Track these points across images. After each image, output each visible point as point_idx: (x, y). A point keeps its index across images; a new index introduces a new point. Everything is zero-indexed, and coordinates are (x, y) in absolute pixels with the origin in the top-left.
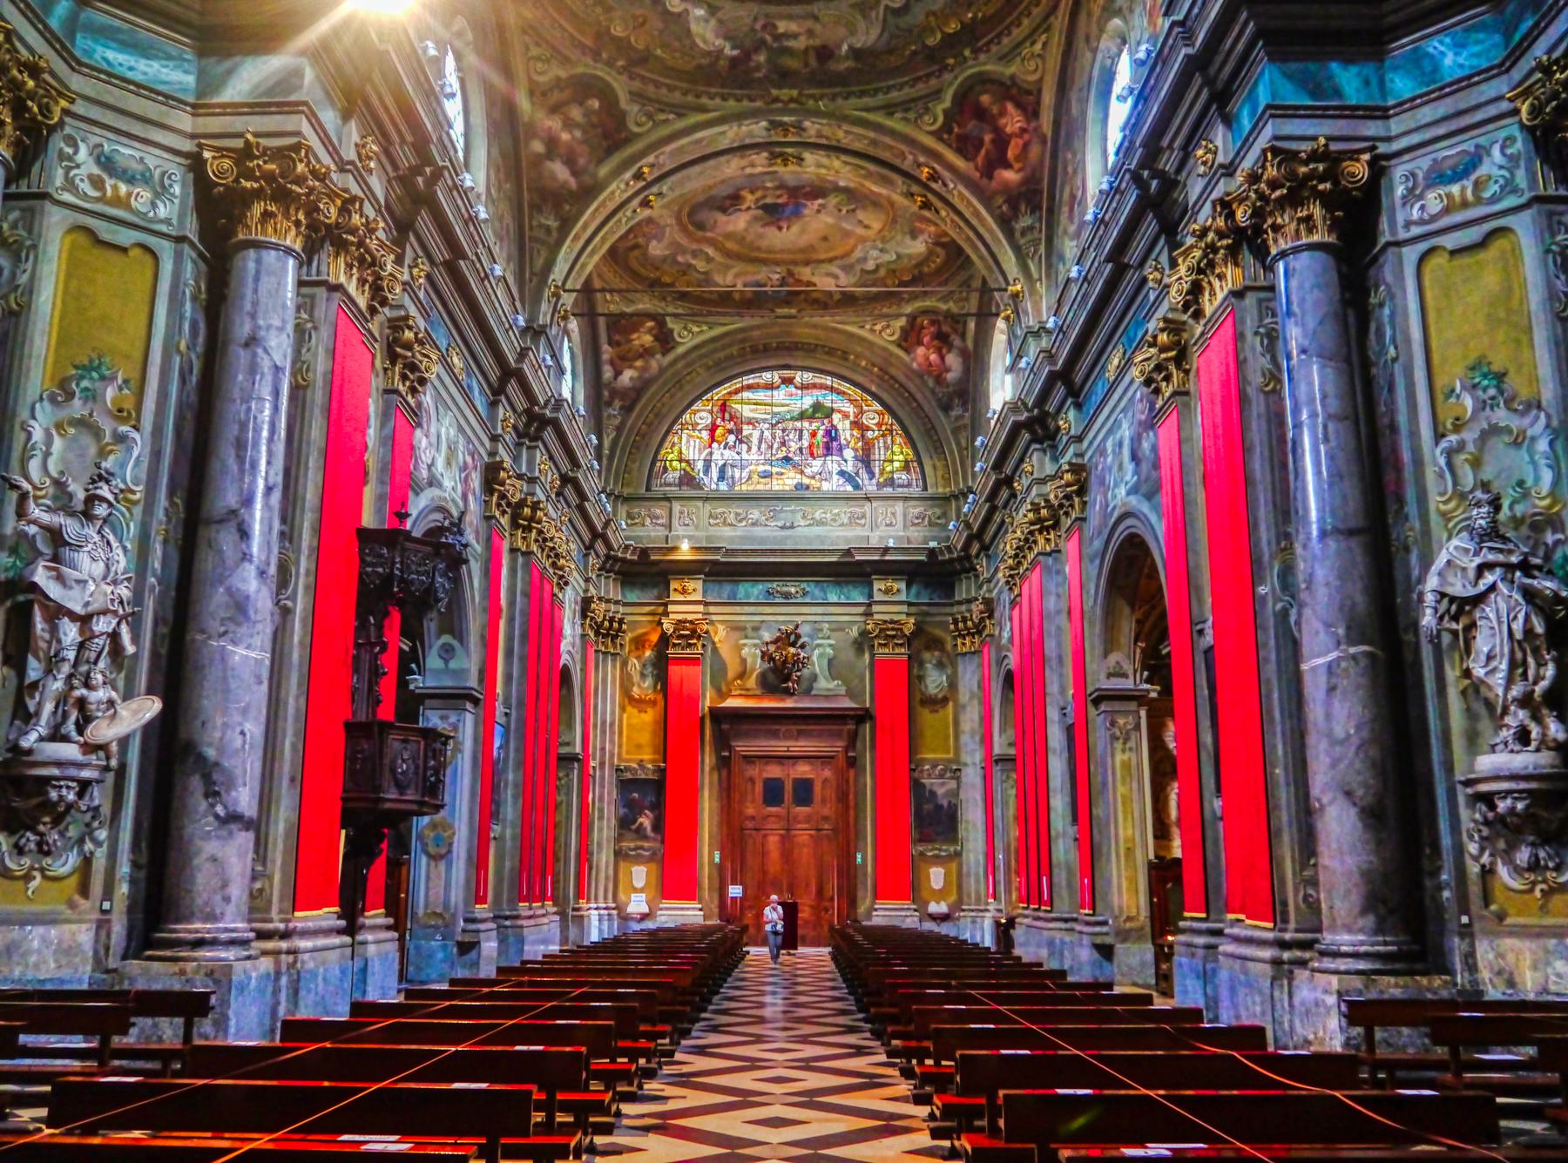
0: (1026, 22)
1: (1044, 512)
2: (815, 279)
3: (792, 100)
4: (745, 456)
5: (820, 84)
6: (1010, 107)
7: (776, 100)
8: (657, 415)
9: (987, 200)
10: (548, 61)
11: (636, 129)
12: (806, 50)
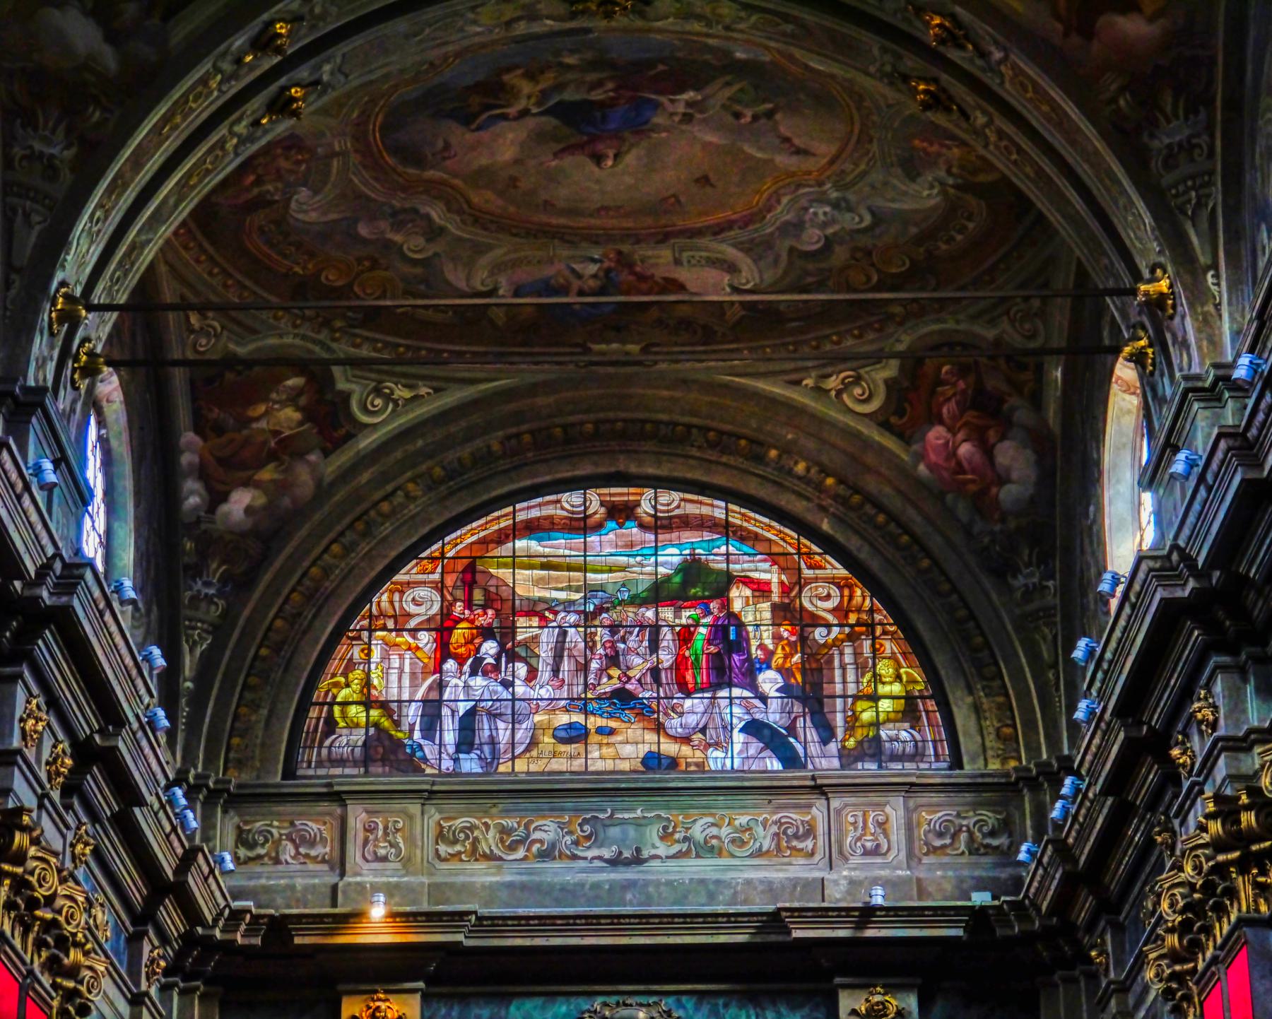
1: (1248, 819)
2: (683, 274)
4: (520, 689)
8: (309, 597)
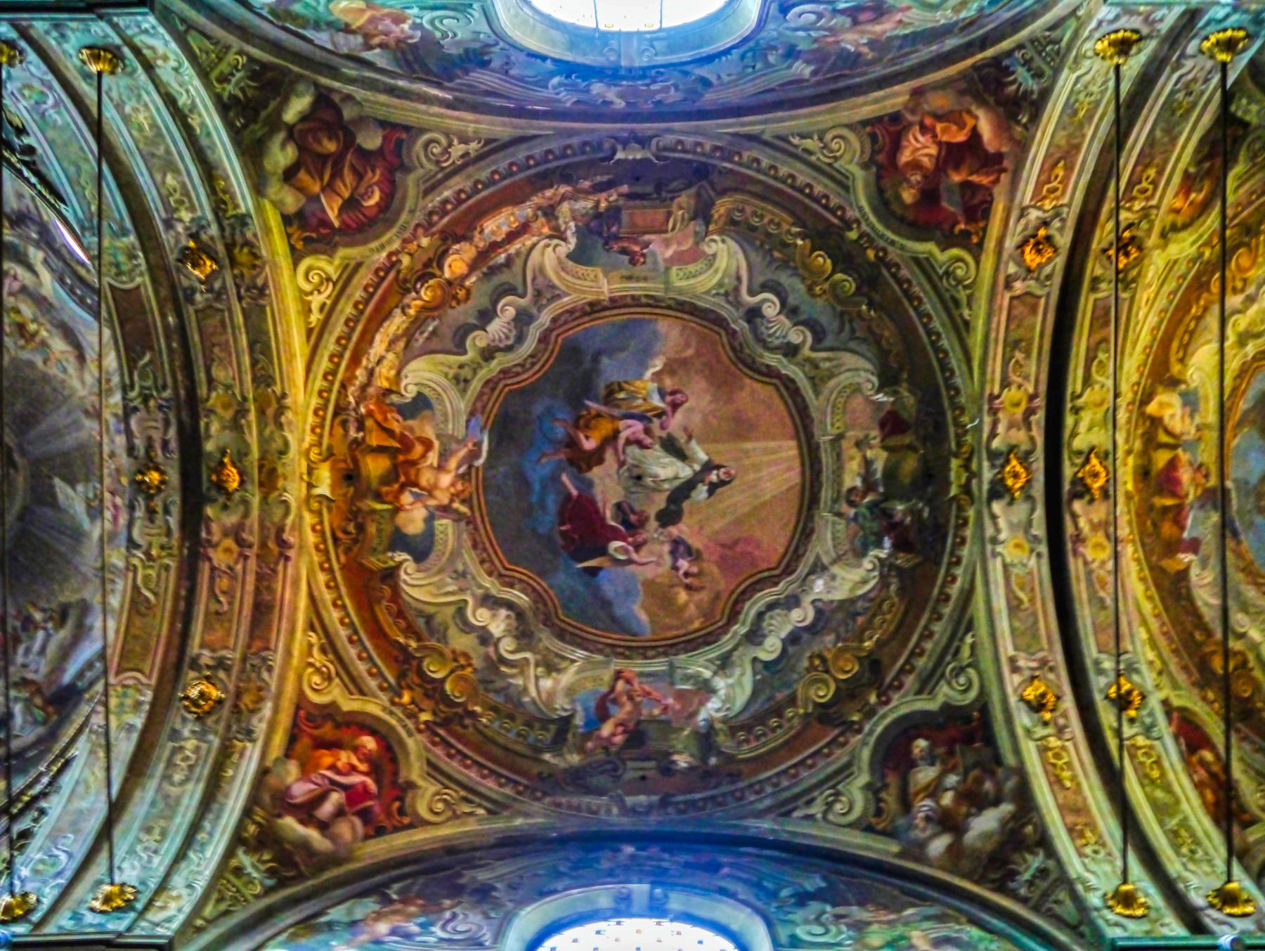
0: (784, 171)
3: (966, 466)
5: (940, 427)
6: (905, 157)
7: (966, 489)
9: (1023, 147)
10: (837, 794)
11: (973, 694)
12: (885, 448)
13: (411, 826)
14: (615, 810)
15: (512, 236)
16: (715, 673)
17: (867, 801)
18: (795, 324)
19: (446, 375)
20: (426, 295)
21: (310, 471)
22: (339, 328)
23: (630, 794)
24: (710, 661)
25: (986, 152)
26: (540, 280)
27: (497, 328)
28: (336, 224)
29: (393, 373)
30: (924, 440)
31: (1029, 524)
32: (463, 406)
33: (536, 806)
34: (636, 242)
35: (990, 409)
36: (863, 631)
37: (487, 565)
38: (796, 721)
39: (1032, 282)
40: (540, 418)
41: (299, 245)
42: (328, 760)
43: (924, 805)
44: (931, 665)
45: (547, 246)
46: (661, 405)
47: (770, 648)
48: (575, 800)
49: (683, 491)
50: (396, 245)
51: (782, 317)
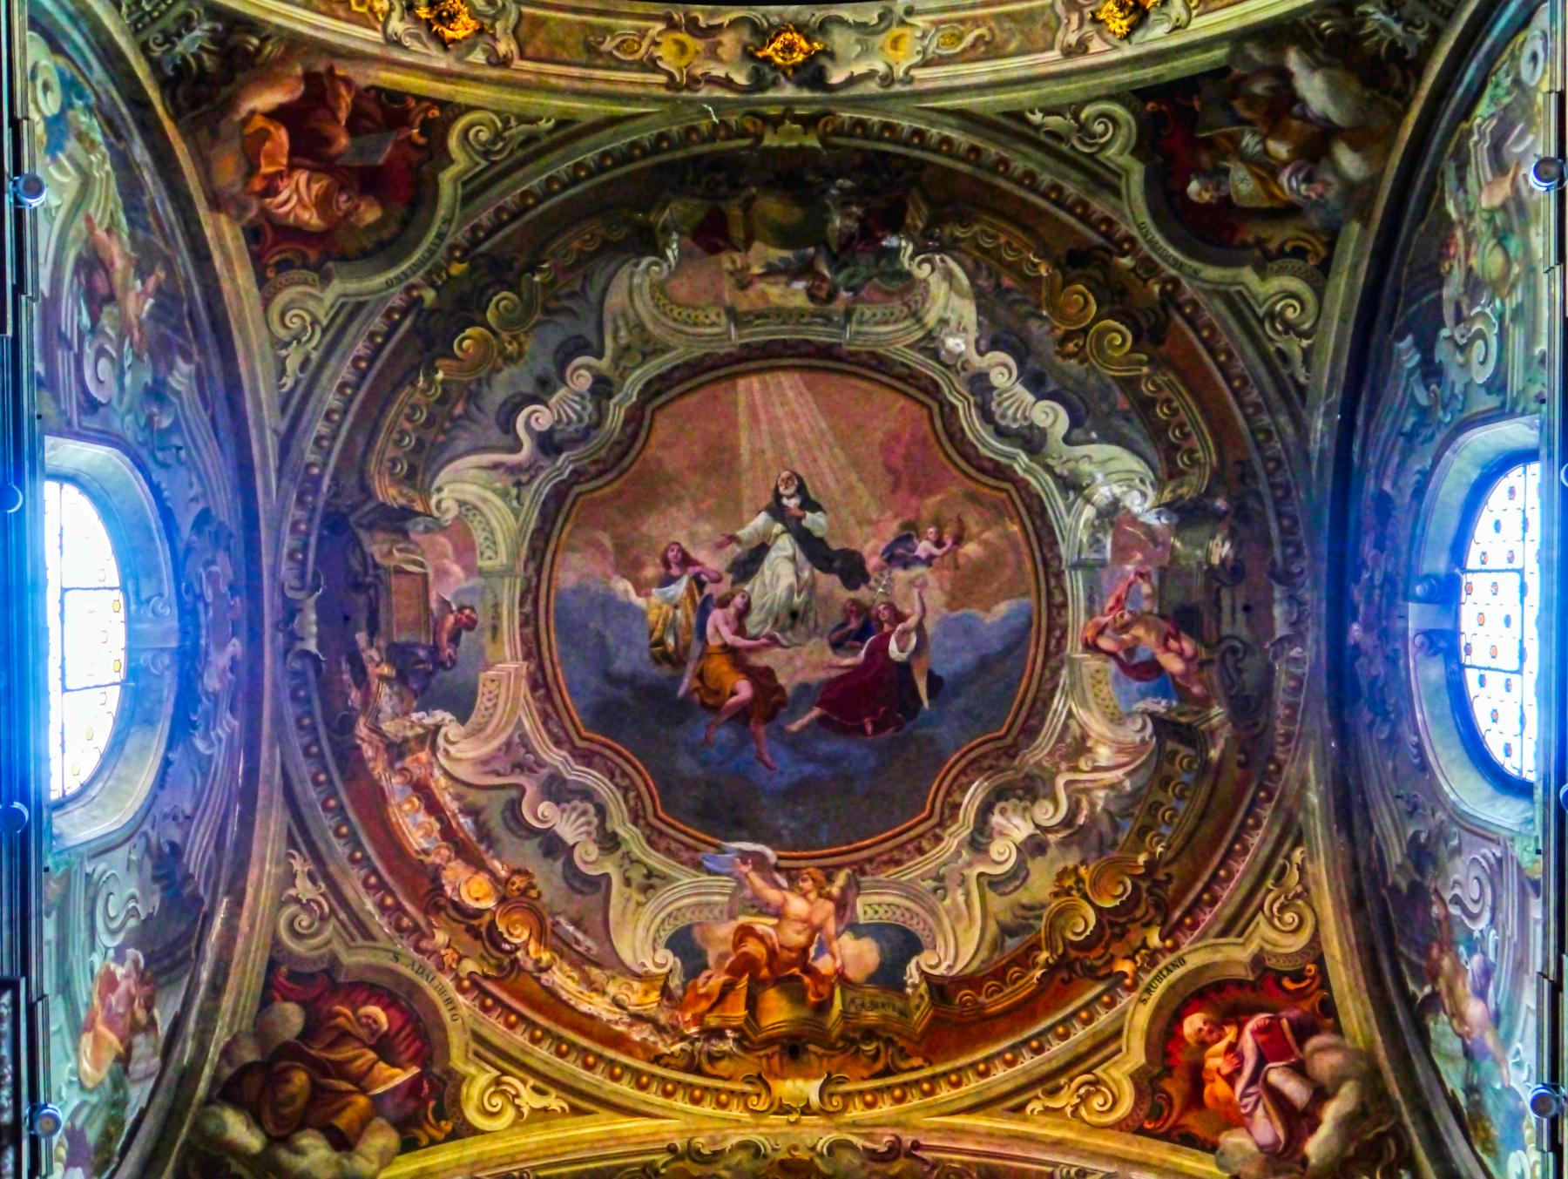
0: (332, 400)
3: (776, 122)
5: (717, 162)
6: (311, 218)
7: (809, 122)
9: (295, 44)
10: (1272, 316)
12: (747, 246)
13: (1320, 961)
14: (1296, 652)
15: (433, 807)
16: (1088, 501)
17: (1280, 272)
18: (563, 381)
19: (639, 904)
20: (520, 935)
21: (784, 1110)
22: (571, 1067)
23: (1271, 631)
24: (1069, 510)
25: (303, 98)
26: (497, 766)
27: (569, 827)
28: (415, 1070)
29: (636, 985)
30: (736, 187)
31: (861, 27)
32: (686, 879)
33: (1290, 771)
34: (443, 618)
35: (687, 87)
36: (1026, 278)
37: (925, 844)
38: (1160, 379)
39: (498, 26)
40: (704, 764)
41: (447, 1126)
42: (1219, 1088)
43: (1289, 184)
44: (1074, 175)
45: (447, 752)
46: (685, 580)
47: (1051, 417)
48: (1282, 711)
49: (813, 548)
50: (447, 981)
51: (553, 401)
